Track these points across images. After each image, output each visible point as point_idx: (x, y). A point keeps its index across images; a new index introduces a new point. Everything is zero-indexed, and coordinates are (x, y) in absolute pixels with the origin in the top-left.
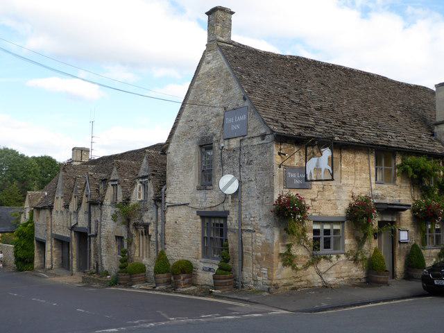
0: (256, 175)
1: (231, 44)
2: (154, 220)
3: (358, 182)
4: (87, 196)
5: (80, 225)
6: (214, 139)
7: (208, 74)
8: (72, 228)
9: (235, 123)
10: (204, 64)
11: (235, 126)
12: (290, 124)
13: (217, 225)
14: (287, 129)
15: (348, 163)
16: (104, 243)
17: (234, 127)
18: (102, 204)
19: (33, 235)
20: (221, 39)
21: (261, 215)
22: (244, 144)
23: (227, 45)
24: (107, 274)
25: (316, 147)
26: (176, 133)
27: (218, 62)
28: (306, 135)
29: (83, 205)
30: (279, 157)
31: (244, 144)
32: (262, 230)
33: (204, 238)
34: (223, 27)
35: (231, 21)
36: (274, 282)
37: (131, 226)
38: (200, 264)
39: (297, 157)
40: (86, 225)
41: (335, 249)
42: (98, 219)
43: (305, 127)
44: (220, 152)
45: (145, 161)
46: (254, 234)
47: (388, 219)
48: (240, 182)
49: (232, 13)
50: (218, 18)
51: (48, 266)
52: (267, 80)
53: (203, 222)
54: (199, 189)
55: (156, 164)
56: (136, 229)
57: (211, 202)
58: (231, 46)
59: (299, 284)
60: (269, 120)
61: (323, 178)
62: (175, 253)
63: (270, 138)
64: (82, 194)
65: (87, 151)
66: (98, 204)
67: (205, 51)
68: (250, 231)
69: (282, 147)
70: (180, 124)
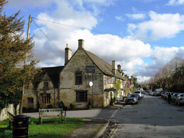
10: (77, 53)
68: (96, 95)
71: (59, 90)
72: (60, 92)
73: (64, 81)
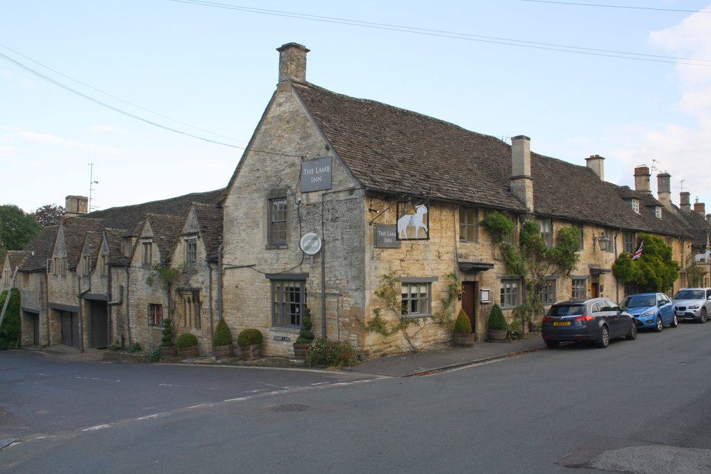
0: (342, 234)
1: (306, 85)
2: (207, 283)
3: (443, 240)
4: (103, 256)
5: (93, 292)
6: (289, 192)
7: (280, 118)
8: (81, 296)
9: (315, 175)
10: (274, 106)
11: (315, 174)
12: (377, 178)
13: (292, 289)
14: (378, 184)
15: (434, 220)
16: (133, 312)
17: (314, 180)
18: (129, 266)
19: (18, 305)
20: (295, 79)
21: (350, 277)
22: (329, 199)
23: (301, 86)
24: (138, 348)
25: (410, 204)
26: (236, 184)
27: (294, 104)
28: (397, 190)
29: (98, 267)
30: (369, 213)
31: (328, 198)
32: (351, 293)
33: (274, 304)
34: (297, 66)
35: (306, 59)
36: (366, 349)
37: (173, 293)
38: (270, 334)
39: (387, 214)
40: (104, 291)
41: (421, 312)
42: (124, 284)
43: (394, 181)
44: (296, 206)
45: (191, 215)
46: (340, 298)
47: (470, 279)
48: (323, 241)
49: (307, 51)
50: (292, 54)
51: (43, 342)
52: (347, 127)
53: (273, 287)
54: (268, 248)
55: (205, 219)
56: (181, 295)
57: (285, 264)
58: (307, 87)
59: (389, 349)
60: (358, 173)
61: (417, 237)
62: (238, 323)
63: (359, 193)
64: (97, 255)
65: (85, 200)
66: (124, 266)
67: (276, 92)
68: (335, 295)
69: (373, 203)
70: (242, 173)
71: (221, 275)
72: (226, 284)
73: (234, 233)
